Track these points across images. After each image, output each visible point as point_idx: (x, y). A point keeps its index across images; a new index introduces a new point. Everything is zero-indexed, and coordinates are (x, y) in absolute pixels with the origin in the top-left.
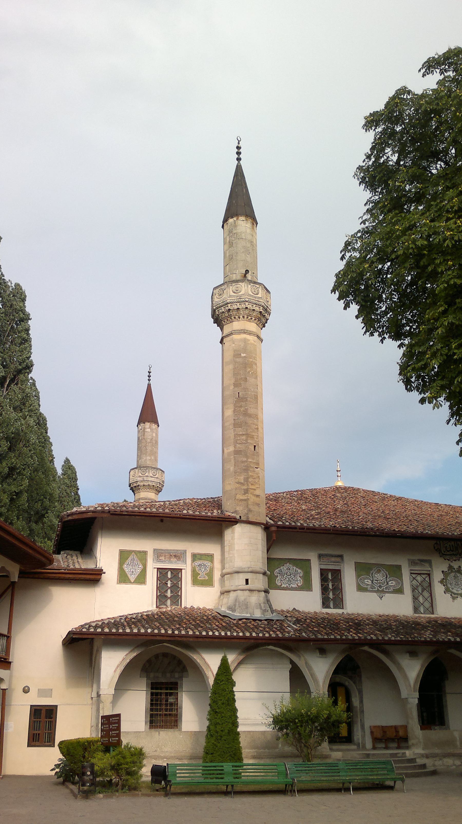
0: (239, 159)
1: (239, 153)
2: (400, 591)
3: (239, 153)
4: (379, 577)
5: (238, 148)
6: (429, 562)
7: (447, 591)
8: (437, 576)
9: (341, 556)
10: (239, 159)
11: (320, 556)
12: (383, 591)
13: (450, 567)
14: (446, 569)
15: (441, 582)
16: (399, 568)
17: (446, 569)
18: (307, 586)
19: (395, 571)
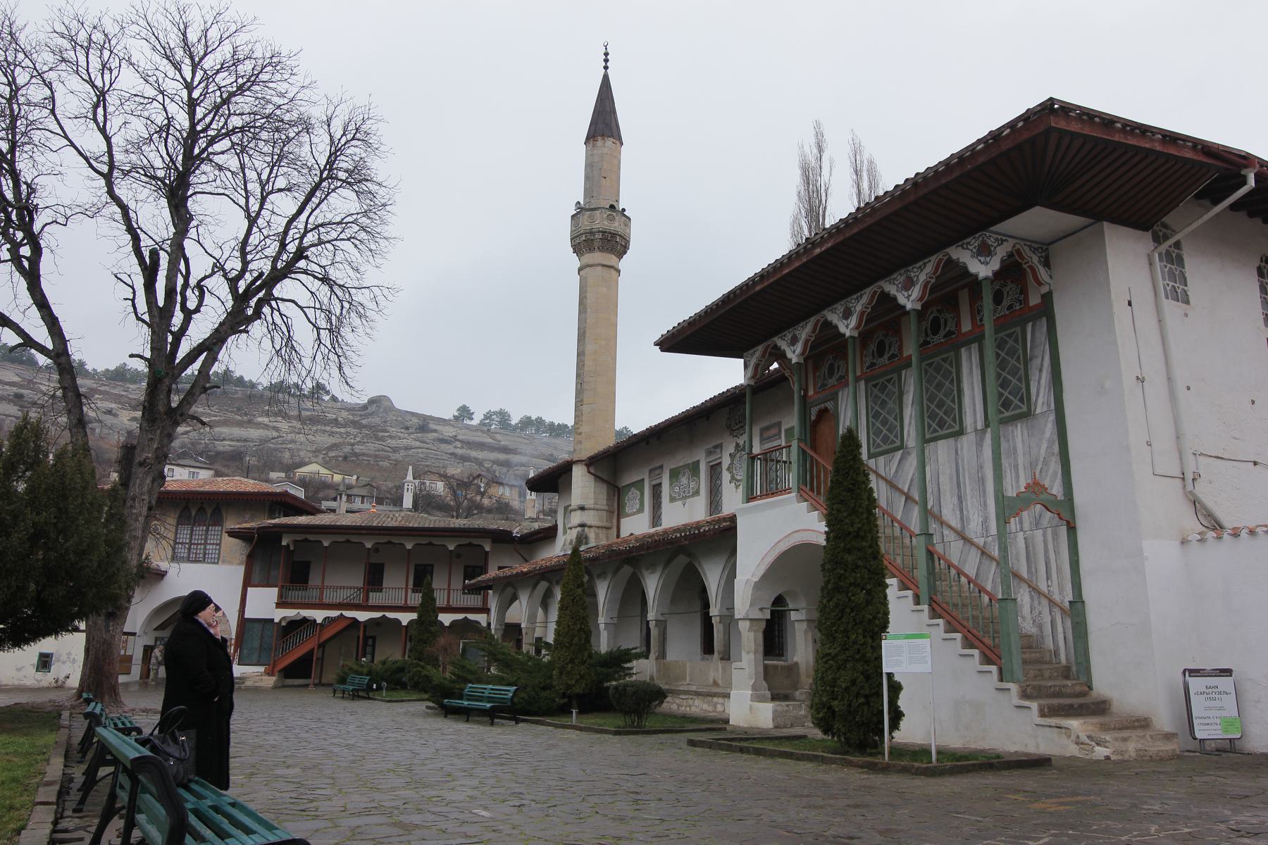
0: (606, 68)
1: (606, 61)
2: (697, 493)
3: (606, 61)
4: (684, 480)
5: (606, 54)
6: (720, 446)
7: (733, 479)
8: (726, 461)
9: (661, 467)
10: (606, 68)
11: (650, 471)
12: (685, 498)
13: (737, 445)
14: (732, 451)
15: (728, 469)
16: (697, 464)
17: (732, 451)
18: (641, 510)
19: (695, 468)
